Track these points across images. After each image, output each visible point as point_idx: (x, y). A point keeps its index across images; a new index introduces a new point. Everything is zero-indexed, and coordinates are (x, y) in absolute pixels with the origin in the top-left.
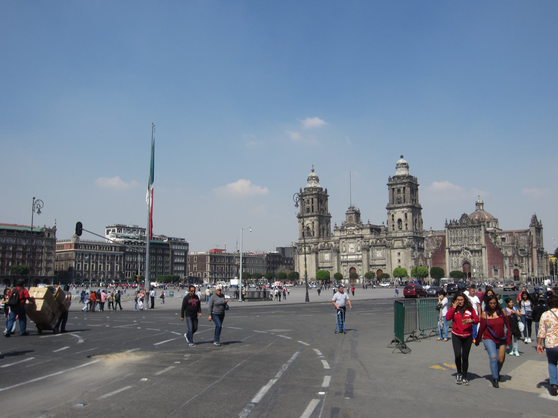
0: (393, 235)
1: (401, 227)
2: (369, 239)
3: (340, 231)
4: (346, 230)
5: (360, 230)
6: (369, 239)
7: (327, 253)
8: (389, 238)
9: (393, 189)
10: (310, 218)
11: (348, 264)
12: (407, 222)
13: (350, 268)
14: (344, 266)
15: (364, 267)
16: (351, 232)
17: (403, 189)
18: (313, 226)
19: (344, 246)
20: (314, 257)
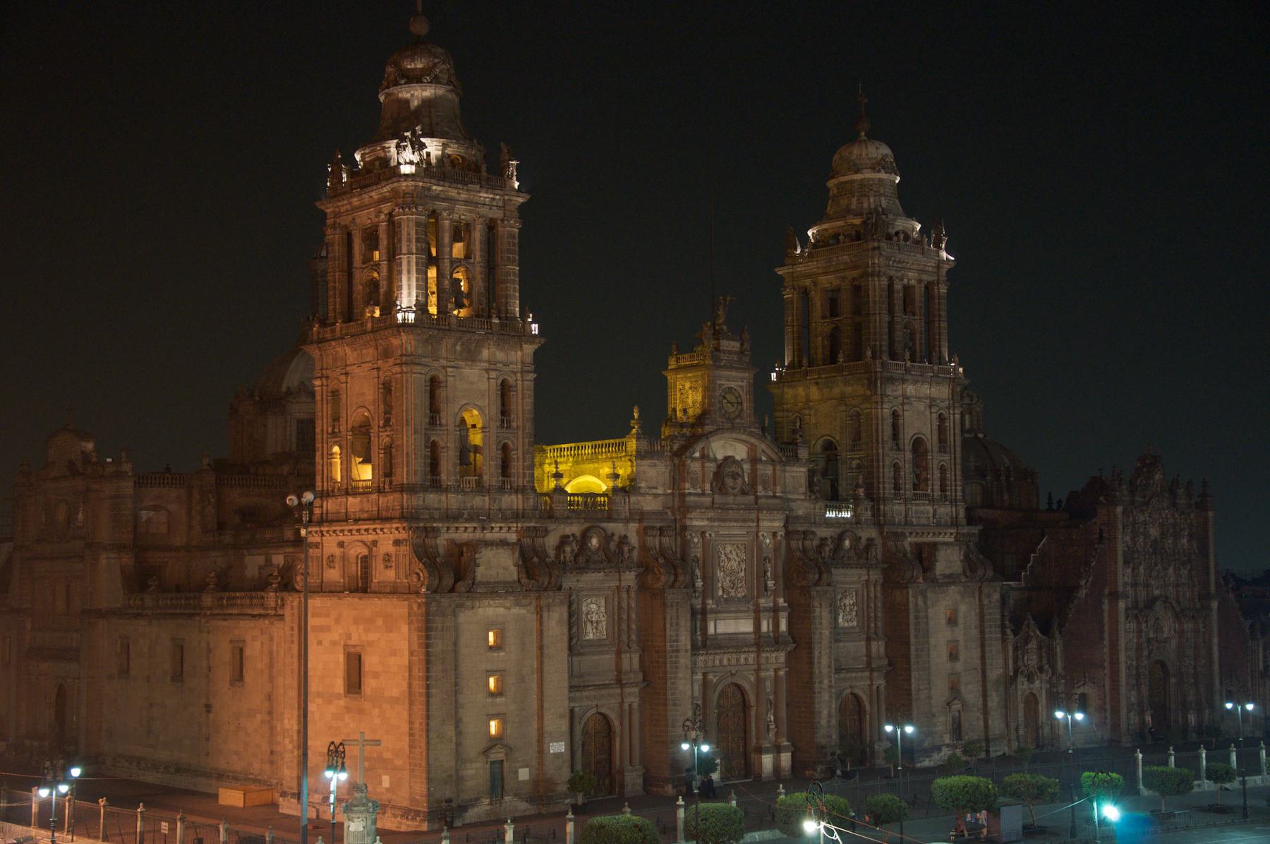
13: (720, 688)
15: (821, 682)
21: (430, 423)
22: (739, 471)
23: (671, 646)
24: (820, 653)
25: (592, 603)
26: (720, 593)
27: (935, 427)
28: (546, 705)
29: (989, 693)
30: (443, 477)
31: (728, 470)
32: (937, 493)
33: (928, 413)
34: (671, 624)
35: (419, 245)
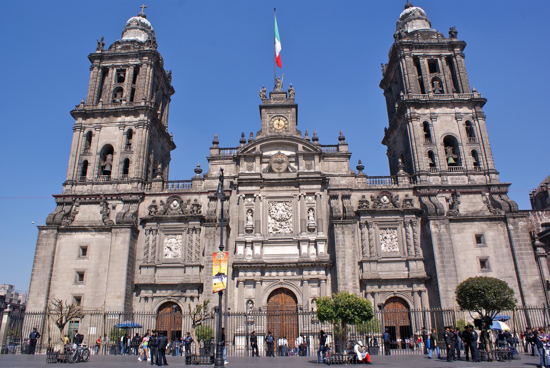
0: (434, 180)
1: (451, 161)
2: (352, 190)
3: (237, 160)
4: (261, 157)
5: (317, 159)
6: (352, 190)
7: (176, 232)
8: (428, 187)
9: (416, 60)
10: (119, 119)
11: (263, 274)
12: (474, 147)
14: (246, 282)
15: (345, 284)
16: (280, 162)
17: (444, 60)
18: (129, 145)
19: (250, 211)
20: (123, 242)
21: (84, 152)
22: (284, 159)
23: (208, 258)
24: (344, 264)
25: (172, 238)
26: (271, 230)
27: (463, 128)
28: (108, 290)
29: (525, 294)
30: (87, 176)
31: (275, 159)
32: (471, 167)
33: (456, 121)
34: (209, 245)
35: (93, 80)
